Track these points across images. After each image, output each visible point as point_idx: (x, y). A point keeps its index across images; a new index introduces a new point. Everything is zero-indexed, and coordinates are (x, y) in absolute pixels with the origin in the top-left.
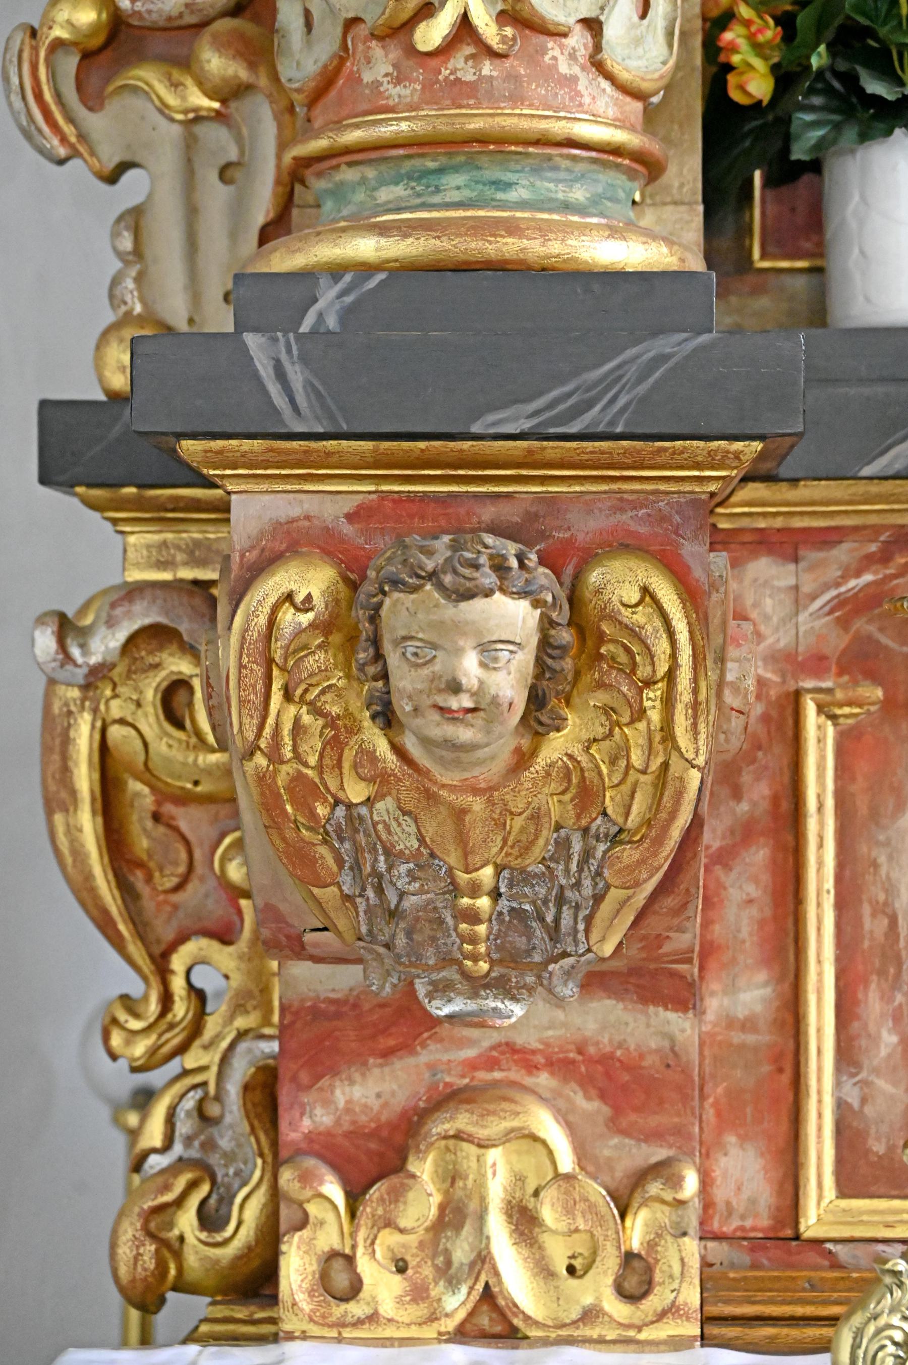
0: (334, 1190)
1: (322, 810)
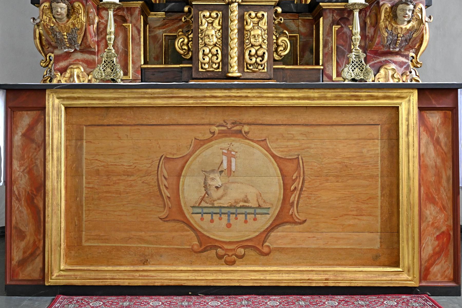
0: (59, 74)
1: (49, 27)
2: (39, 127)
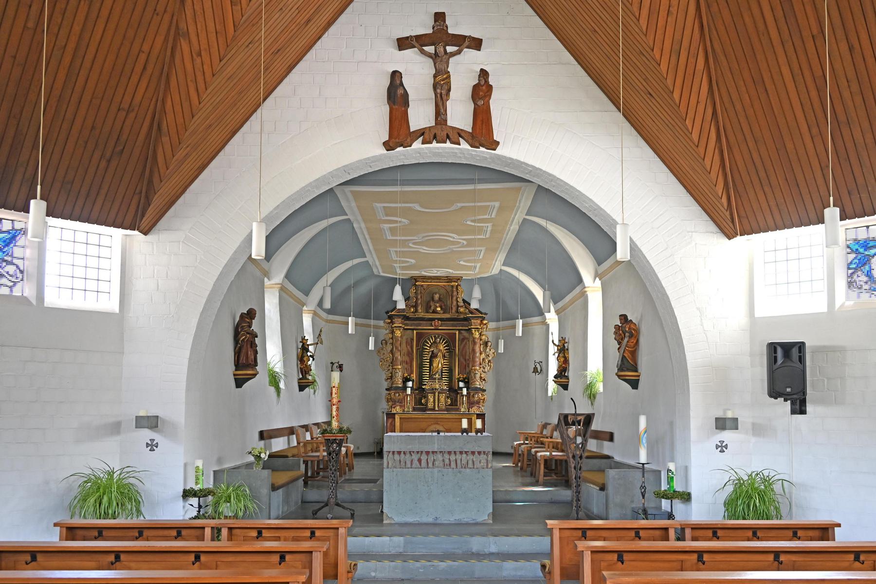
2: (394, 422)
